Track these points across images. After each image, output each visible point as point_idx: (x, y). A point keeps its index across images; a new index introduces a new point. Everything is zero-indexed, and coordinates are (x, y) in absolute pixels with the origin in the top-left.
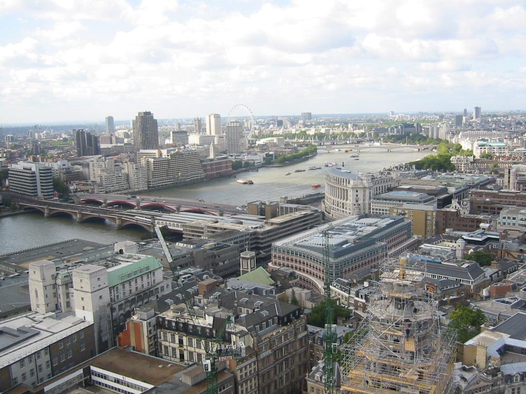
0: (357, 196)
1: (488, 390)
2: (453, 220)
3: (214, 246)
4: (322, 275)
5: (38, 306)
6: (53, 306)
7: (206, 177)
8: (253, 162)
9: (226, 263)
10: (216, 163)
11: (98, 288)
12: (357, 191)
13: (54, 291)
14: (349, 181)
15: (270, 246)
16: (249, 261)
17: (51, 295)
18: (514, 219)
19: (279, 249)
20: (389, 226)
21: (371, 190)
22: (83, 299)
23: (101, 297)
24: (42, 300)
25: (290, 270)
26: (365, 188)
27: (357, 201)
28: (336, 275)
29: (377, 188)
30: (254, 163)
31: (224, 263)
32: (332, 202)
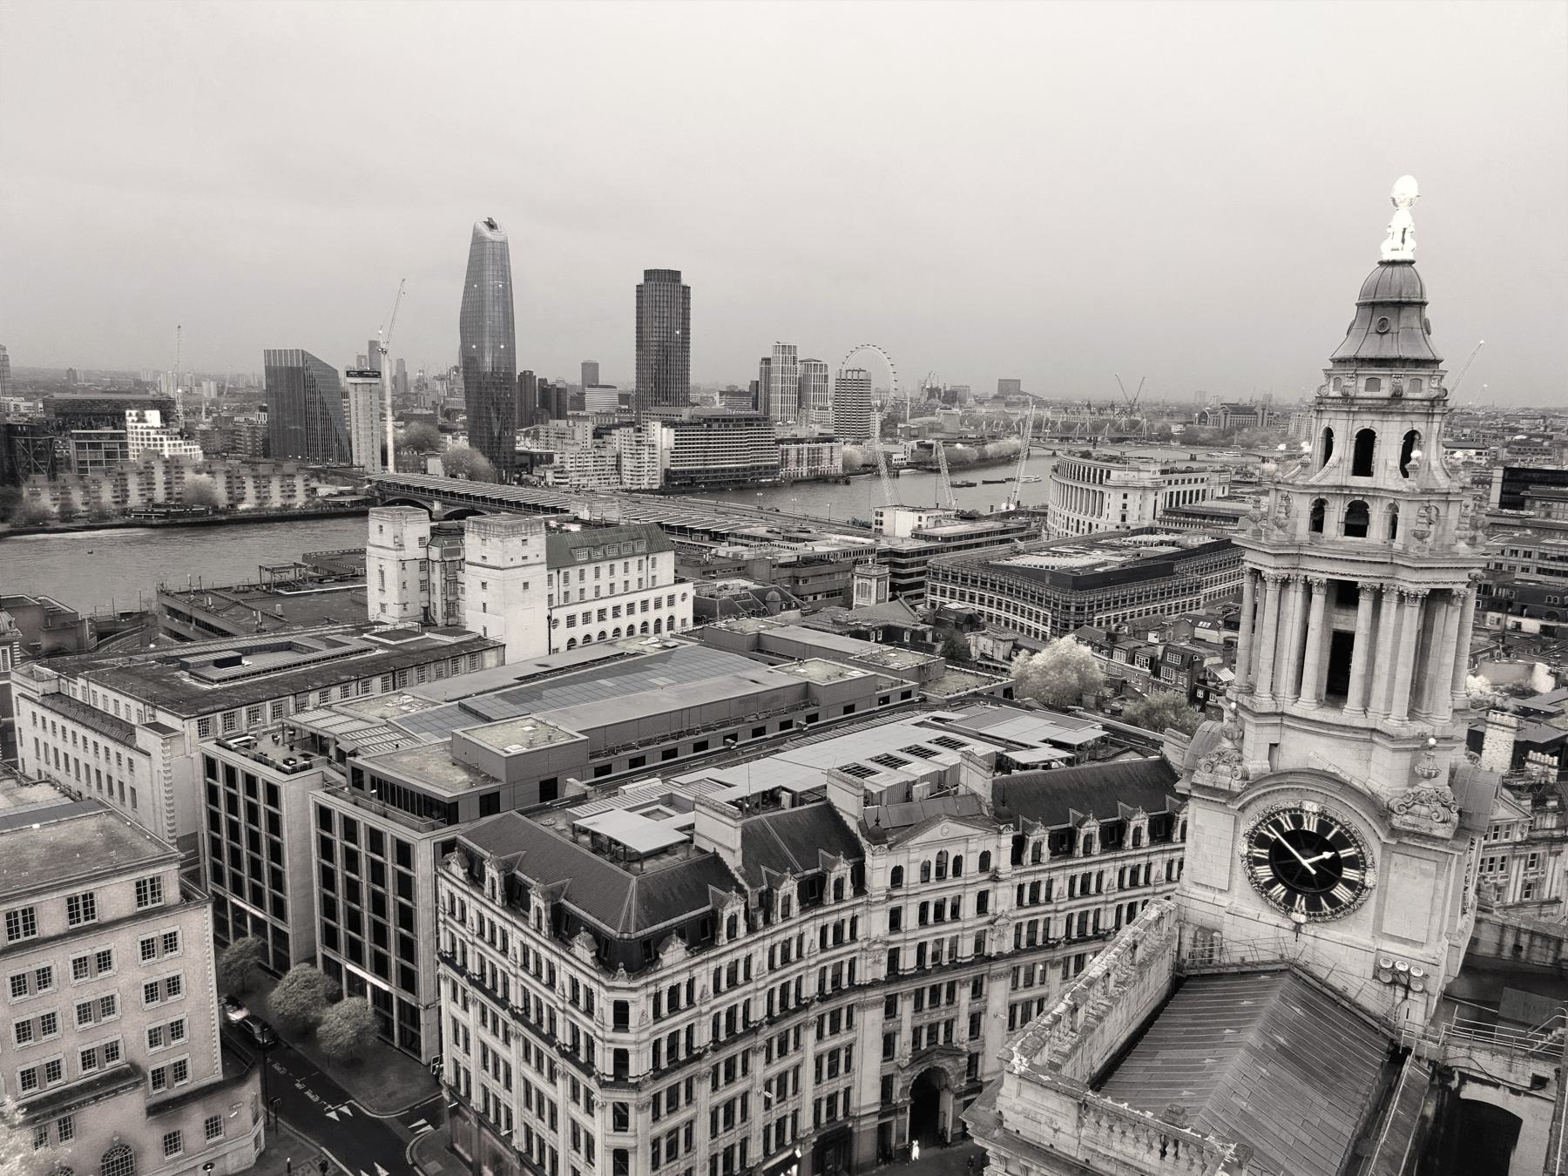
0: (1125, 506)
1: (1518, 838)
3: (795, 559)
5: (383, 606)
6: (415, 609)
9: (819, 597)
11: (521, 562)
12: (1125, 496)
13: (423, 576)
14: (1109, 472)
16: (875, 581)
17: (414, 586)
18: (1528, 554)
21: (1159, 496)
22: (484, 584)
23: (526, 585)
24: (392, 596)
26: (1145, 488)
27: (1124, 518)
28: (1077, 608)
29: (1172, 493)
31: (815, 598)
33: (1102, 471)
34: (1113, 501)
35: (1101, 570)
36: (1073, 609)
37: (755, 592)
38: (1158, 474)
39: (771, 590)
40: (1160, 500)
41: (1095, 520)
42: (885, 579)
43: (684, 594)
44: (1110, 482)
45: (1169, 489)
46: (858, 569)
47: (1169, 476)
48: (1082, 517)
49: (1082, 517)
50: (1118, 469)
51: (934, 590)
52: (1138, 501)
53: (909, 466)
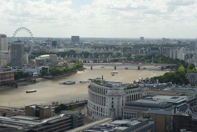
0: (113, 102)
2: (187, 122)
8: (31, 73)
12: (113, 99)
14: (107, 90)
20: (137, 126)
21: (124, 98)
26: (119, 96)
27: (112, 106)
29: (128, 96)
30: (32, 74)
32: (93, 107)
33: (104, 90)
34: (109, 101)
38: (123, 91)
40: (124, 99)
41: (103, 107)
44: (107, 94)
45: (127, 96)
48: (99, 106)
49: (99, 106)
50: (110, 89)
53: (39, 76)
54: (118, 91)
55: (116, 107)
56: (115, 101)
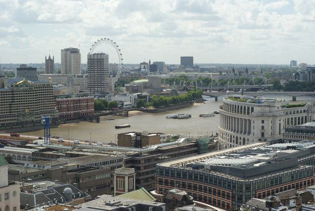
0: (263, 127)
3: (76, 168)
4: (230, 202)
7: (61, 117)
8: (121, 103)
10: (74, 101)
12: (263, 122)
14: (252, 108)
15: (154, 165)
16: (127, 178)
19: (167, 171)
21: (282, 121)
25: (184, 193)
27: (263, 134)
30: (123, 104)
31: (89, 190)
32: (229, 138)
35: (257, 165)
36: (244, 189)
37: (57, 189)
39: (66, 187)
42: (133, 177)
43: (14, 192)
45: (287, 117)
46: (117, 171)
47: (289, 110)
48: (239, 135)
50: (259, 106)
51: (161, 182)
52: (270, 124)
53: (133, 108)
54: (272, 109)
55: (269, 136)
56: (268, 125)
